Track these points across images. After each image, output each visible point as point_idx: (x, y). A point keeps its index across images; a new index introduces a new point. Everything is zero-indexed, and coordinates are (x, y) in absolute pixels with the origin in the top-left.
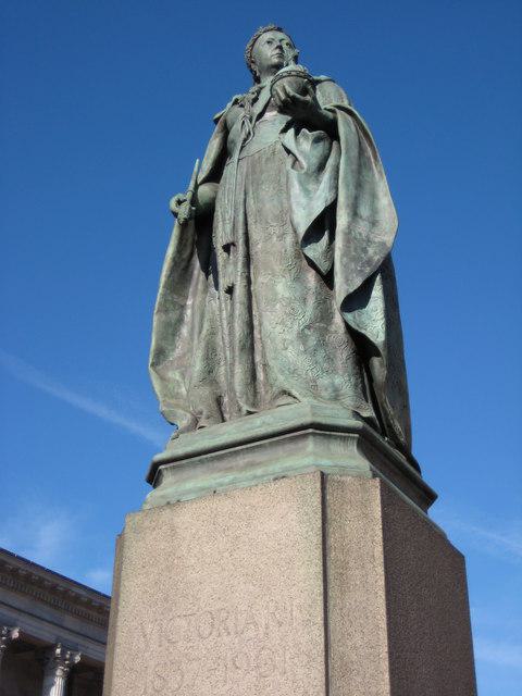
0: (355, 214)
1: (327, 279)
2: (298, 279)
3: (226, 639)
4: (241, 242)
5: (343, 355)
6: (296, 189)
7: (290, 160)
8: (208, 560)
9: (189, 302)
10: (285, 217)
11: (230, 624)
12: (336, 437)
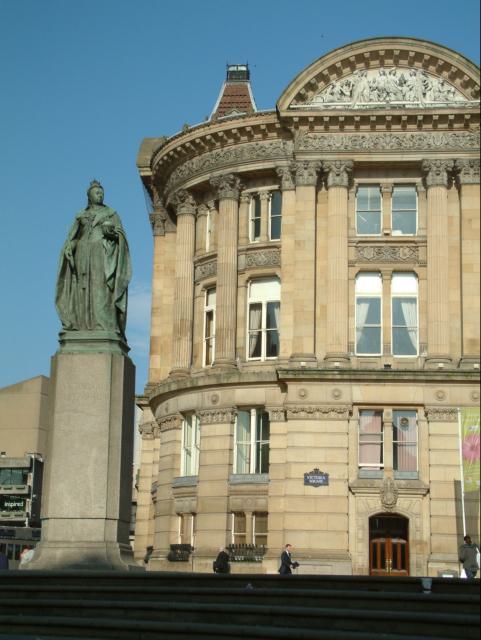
0: (121, 272)
1: (112, 291)
2: (105, 290)
5: (114, 314)
6: (106, 261)
10: (102, 269)
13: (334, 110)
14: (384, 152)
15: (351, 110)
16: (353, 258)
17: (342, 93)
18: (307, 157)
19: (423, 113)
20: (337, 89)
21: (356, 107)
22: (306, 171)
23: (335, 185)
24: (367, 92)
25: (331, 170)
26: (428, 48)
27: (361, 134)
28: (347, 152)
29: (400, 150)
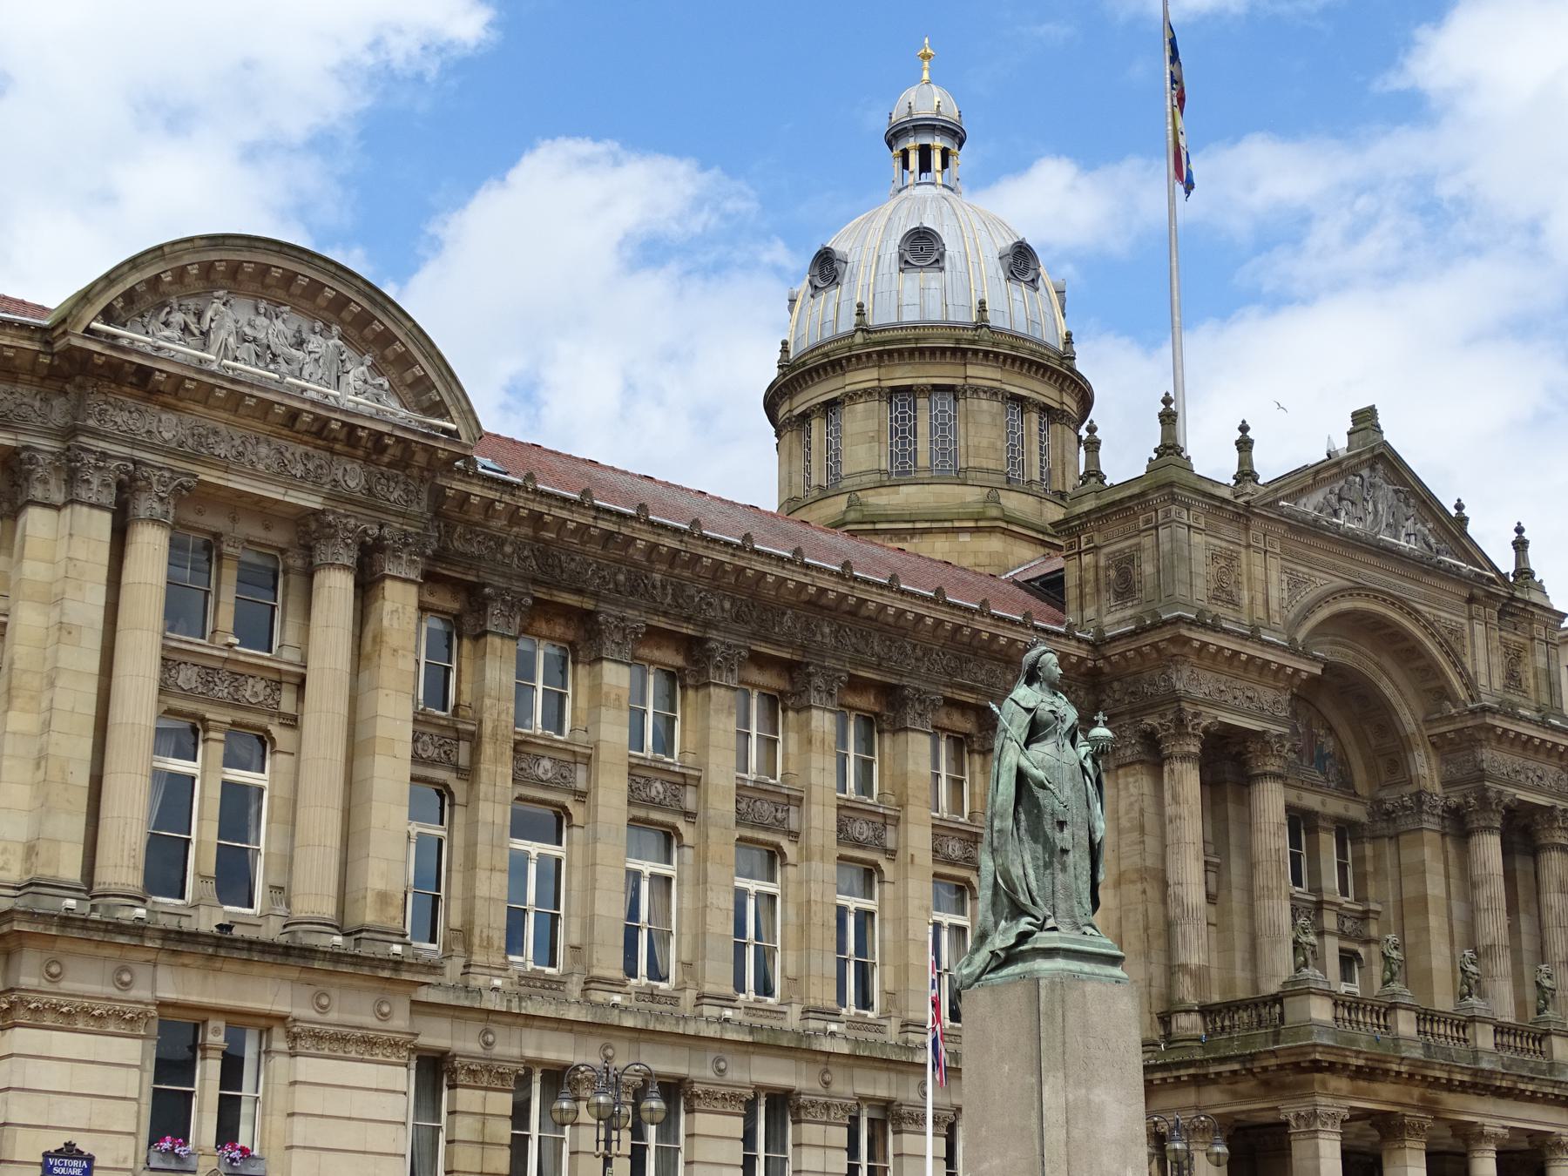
14: (255, 476)
19: (343, 418)
23: (155, 521)
26: (359, 292)
29: (282, 474)
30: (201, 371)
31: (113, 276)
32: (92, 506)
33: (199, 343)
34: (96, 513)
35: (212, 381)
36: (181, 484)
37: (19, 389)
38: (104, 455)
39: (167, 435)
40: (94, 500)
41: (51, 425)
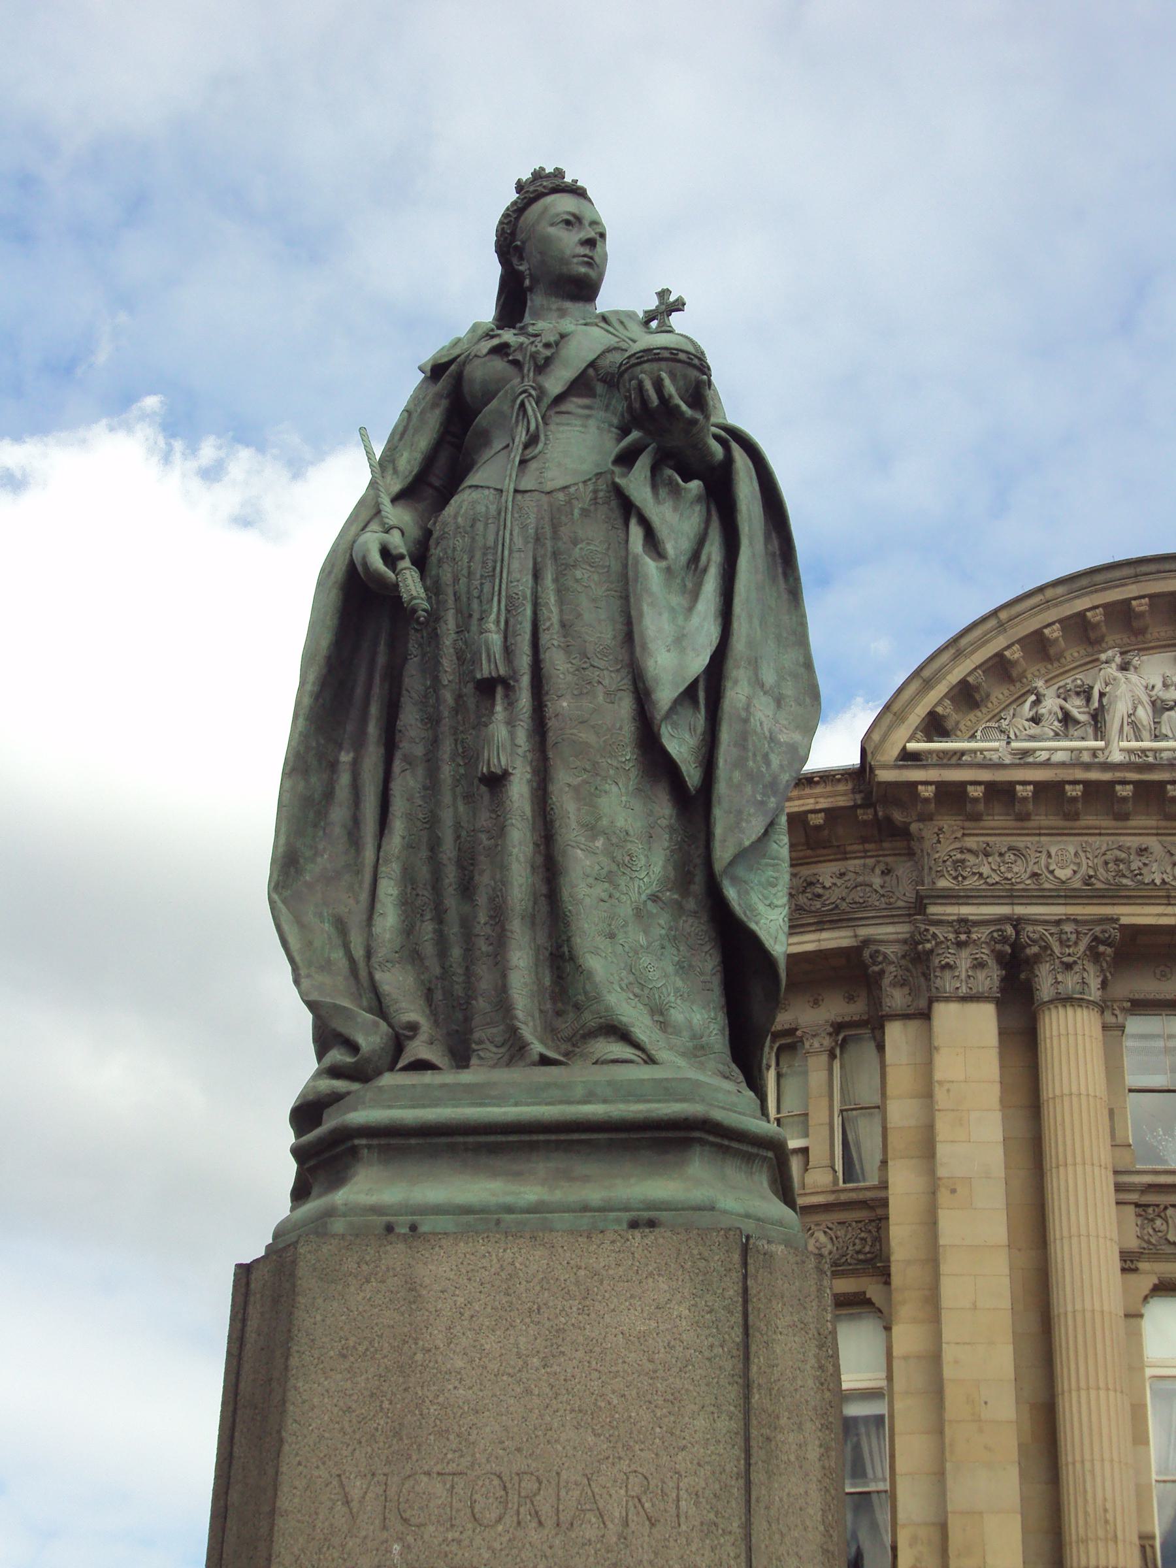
3: (534, 1535)
4: (525, 681)
7: (636, 533)
8: (493, 1366)
9: (345, 757)
11: (546, 1510)
12: (737, 1153)
13: (1047, 764)
15: (1107, 766)
16: (1133, 1244)
17: (1067, 719)
18: (965, 910)
20: (1051, 704)
21: (1117, 757)
22: (965, 953)
23: (1066, 1000)
24: (1144, 715)
25: (1047, 947)
27: (1133, 842)
28: (1090, 893)
30: (1087, 766)
31: (926, 673)
32: (965, 999)
33: (1090, 730)
34: (973, 1008)
35: (1107, 776)
36: (1095, 939)
37: (854, 864)
38: (964, 923)
39: (1063, 874)
40: (964, 990)
41: (901, 904)
